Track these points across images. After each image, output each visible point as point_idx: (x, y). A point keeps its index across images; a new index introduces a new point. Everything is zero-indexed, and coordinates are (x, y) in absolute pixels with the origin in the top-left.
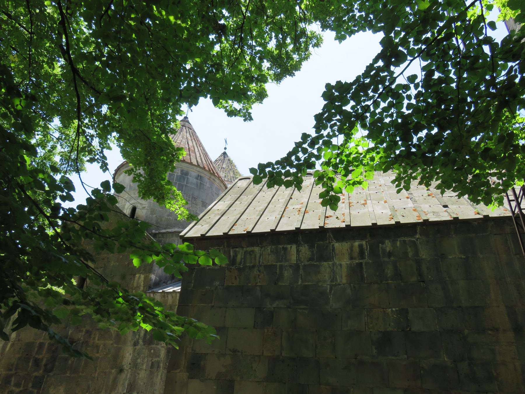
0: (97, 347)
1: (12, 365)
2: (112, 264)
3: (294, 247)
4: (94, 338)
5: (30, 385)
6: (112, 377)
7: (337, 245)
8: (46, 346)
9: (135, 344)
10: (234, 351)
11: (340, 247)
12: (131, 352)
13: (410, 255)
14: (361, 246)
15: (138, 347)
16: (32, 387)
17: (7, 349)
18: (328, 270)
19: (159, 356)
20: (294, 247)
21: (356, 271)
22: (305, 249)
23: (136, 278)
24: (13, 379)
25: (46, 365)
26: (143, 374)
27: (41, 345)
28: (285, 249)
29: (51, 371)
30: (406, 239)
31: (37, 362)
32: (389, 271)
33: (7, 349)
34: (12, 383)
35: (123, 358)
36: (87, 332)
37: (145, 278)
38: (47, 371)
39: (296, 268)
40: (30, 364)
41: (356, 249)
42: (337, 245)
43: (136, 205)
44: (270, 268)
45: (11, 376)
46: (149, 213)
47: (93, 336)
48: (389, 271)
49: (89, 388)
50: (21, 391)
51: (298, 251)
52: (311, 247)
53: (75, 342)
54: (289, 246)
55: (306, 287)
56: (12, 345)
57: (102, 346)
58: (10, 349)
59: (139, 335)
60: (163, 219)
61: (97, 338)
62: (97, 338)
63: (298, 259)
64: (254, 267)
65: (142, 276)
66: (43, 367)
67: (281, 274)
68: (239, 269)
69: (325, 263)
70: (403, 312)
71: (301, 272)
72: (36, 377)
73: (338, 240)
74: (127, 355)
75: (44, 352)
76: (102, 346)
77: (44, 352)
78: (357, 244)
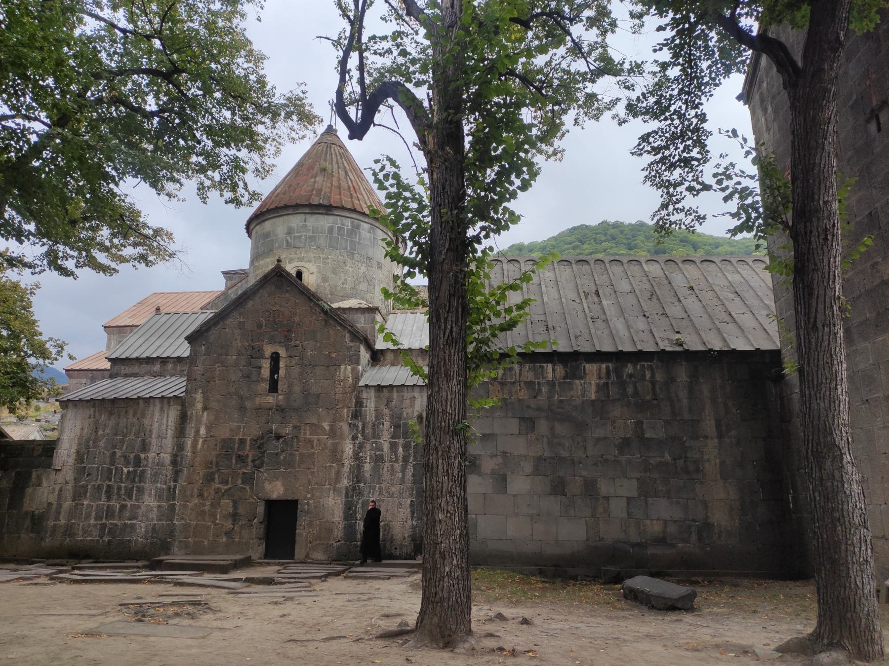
0: (310, 442)
1: (211, 463)
2: (309, 353)
3: (550, 366)
4: (305, 434)
5: (240, 481)
6: (333, 471)
7: (588, 366)
8: (248, 443)
9: (354, 438)
10: (504, 452)
11: (591, 368)
12: (352, 446)
13: (648, 376)
14: (607, 368)
15: (357, 442)
16: (243, 483)
17: (199, 446)
18: (580, 387)
19: (382, 450)
20: (550, 366)
21: (603, 388)
22: (560, 369)
23: (342, 370)
24: (216, 476)
25: (253, 461)
26: (367, 467)
27: (242, 441)
28: (542, 367)
29: (261, 466)
30: (646, 364)
31: (241, 459)
32: (630, 390)
33: (199, 446)
34: (217, 480)
35: (343, 452)
36: (295, 427)
37: (353, 370)
38: (258, 467)
39: (552, 384)
40: (234, 461)
41: (604, 371)
42: (587, 366)
43: (302, 269)
44: (530, 384)
45: (213, 473)
46: (320, 280)
47: (302, 431)
48: (630, 390)
49: (310, 482)
50: (230, 489)
51: (553, 370)
52: (565, 366)
53: (282, 437)
54: (545, 365)
55: (561, 401)
56: (205, 441)
57: (315, 441)
58: (203, 446)
59: (357, 430)
60: (338, 288)
61: (308, 433)
62: (308, 433)
63: (554, 377)
64: (514, 382)
65: (349, 368)
66: (250, 464)
67: (540, 390)
68: (500, 383)
69: (578, 382)
70: (639, 423)
71: (557, 387)
72: (244, 473)
73: (588, 362)
74: (347, 449)
75: (248, 448)
76: (315, 441)
77: (248, 448)
78: (604, 366)
